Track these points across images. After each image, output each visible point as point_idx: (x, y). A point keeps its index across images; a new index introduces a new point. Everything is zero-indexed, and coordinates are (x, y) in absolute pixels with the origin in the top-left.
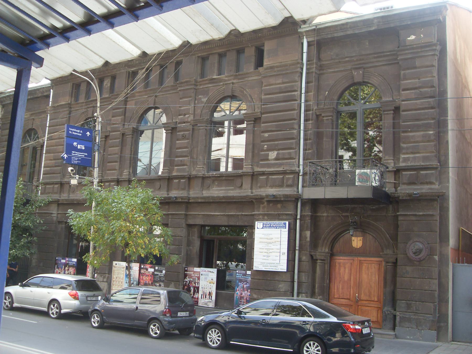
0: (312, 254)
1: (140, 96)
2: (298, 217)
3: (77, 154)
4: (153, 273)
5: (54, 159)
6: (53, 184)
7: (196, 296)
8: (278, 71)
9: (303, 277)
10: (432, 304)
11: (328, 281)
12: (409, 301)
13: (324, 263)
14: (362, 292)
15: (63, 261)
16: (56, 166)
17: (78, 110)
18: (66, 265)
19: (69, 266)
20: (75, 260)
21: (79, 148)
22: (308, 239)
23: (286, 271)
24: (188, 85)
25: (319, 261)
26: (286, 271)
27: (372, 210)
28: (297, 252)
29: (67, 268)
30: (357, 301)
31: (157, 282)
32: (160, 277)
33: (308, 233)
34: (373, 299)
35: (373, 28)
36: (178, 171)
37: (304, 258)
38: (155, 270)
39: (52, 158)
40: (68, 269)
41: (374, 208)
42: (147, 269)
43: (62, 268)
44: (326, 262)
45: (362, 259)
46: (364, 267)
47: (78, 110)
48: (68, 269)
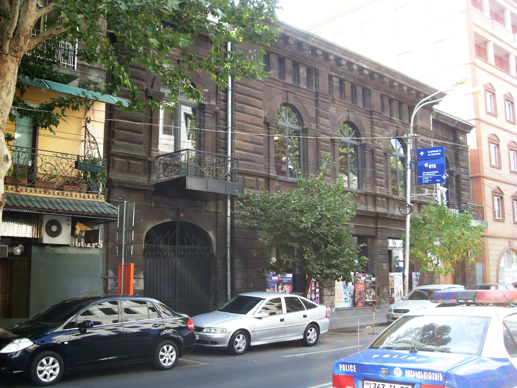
1: (340, 105)
3: (428, 173)
4: (365, 280)
5: (251, 142)
6: (258, 176)
7: (393, 296)
8: (425, 132)
15: (275, 278)
16: (254, 152)
17: (272, 87)
18: (279, 283)
19: (284, 284)
20: (290, 275)
21: (430, 167)
24: (380, 116)
29: (280, 287)
31: (368, 288)
32: (370, 284)
35: (454, 126)
36: (380, 190)
38: (366, 278)
39: (249, 140)
40: (282, 288)
42: (360, 278)
43: (274, 287)
47: (272, 87)
48: (282, 288)
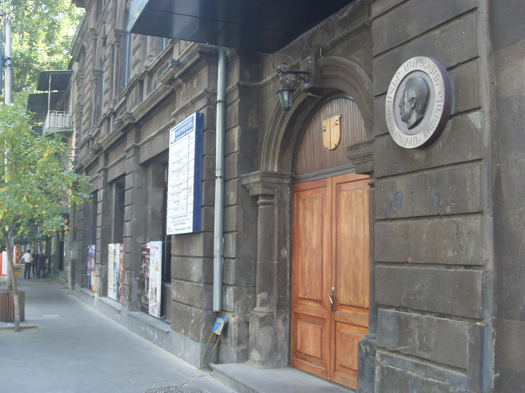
0: (245, 182)
2: (219, 97)
9: (231, 245)
10: (464, 326)
11: (285, 253)
12: (406, 309)
13: (272, 204)
14: (342, 280)
22: (236, 149)
23: (191, 231)
25: (260, 201)
26: (191, 231)
27: (343, 23)
28: (218, 184)
30: (334, 307)
33: (236, 133)
34: (361, 303)
37: (232, 197)
41: (345, 15)
44: (275, 200)
45: (340, 179)
46: (343, 202)
